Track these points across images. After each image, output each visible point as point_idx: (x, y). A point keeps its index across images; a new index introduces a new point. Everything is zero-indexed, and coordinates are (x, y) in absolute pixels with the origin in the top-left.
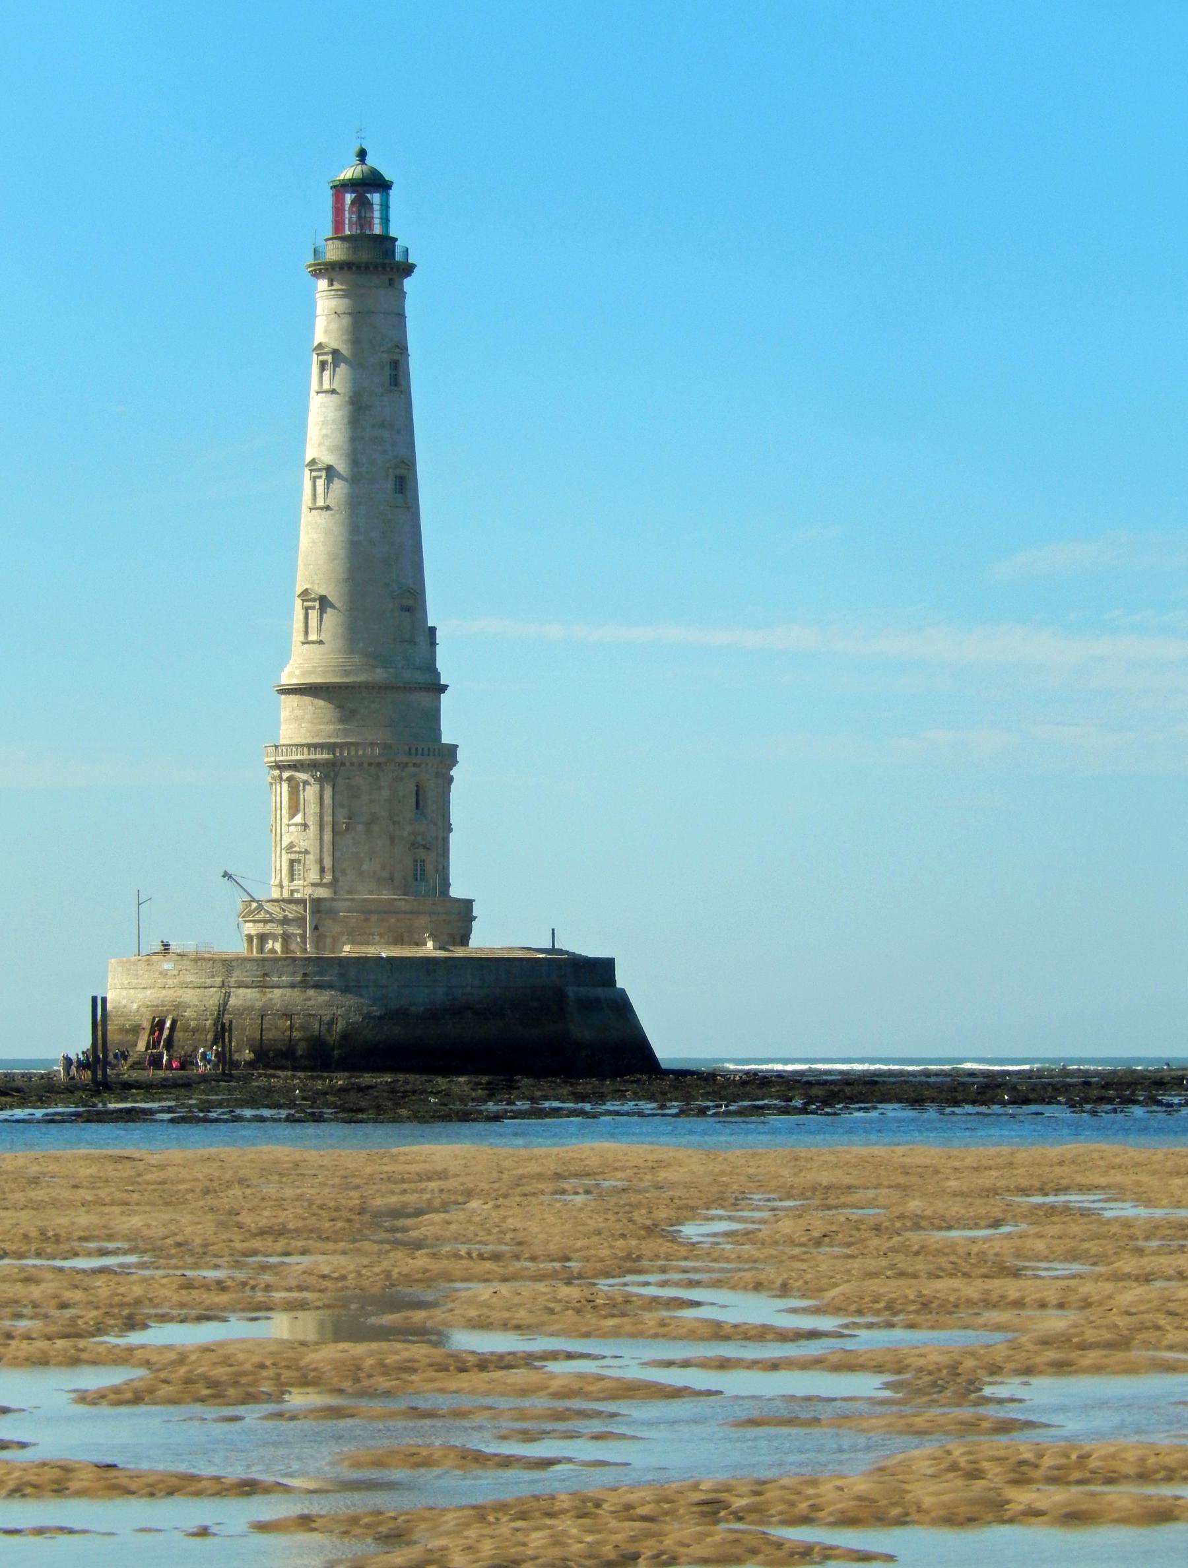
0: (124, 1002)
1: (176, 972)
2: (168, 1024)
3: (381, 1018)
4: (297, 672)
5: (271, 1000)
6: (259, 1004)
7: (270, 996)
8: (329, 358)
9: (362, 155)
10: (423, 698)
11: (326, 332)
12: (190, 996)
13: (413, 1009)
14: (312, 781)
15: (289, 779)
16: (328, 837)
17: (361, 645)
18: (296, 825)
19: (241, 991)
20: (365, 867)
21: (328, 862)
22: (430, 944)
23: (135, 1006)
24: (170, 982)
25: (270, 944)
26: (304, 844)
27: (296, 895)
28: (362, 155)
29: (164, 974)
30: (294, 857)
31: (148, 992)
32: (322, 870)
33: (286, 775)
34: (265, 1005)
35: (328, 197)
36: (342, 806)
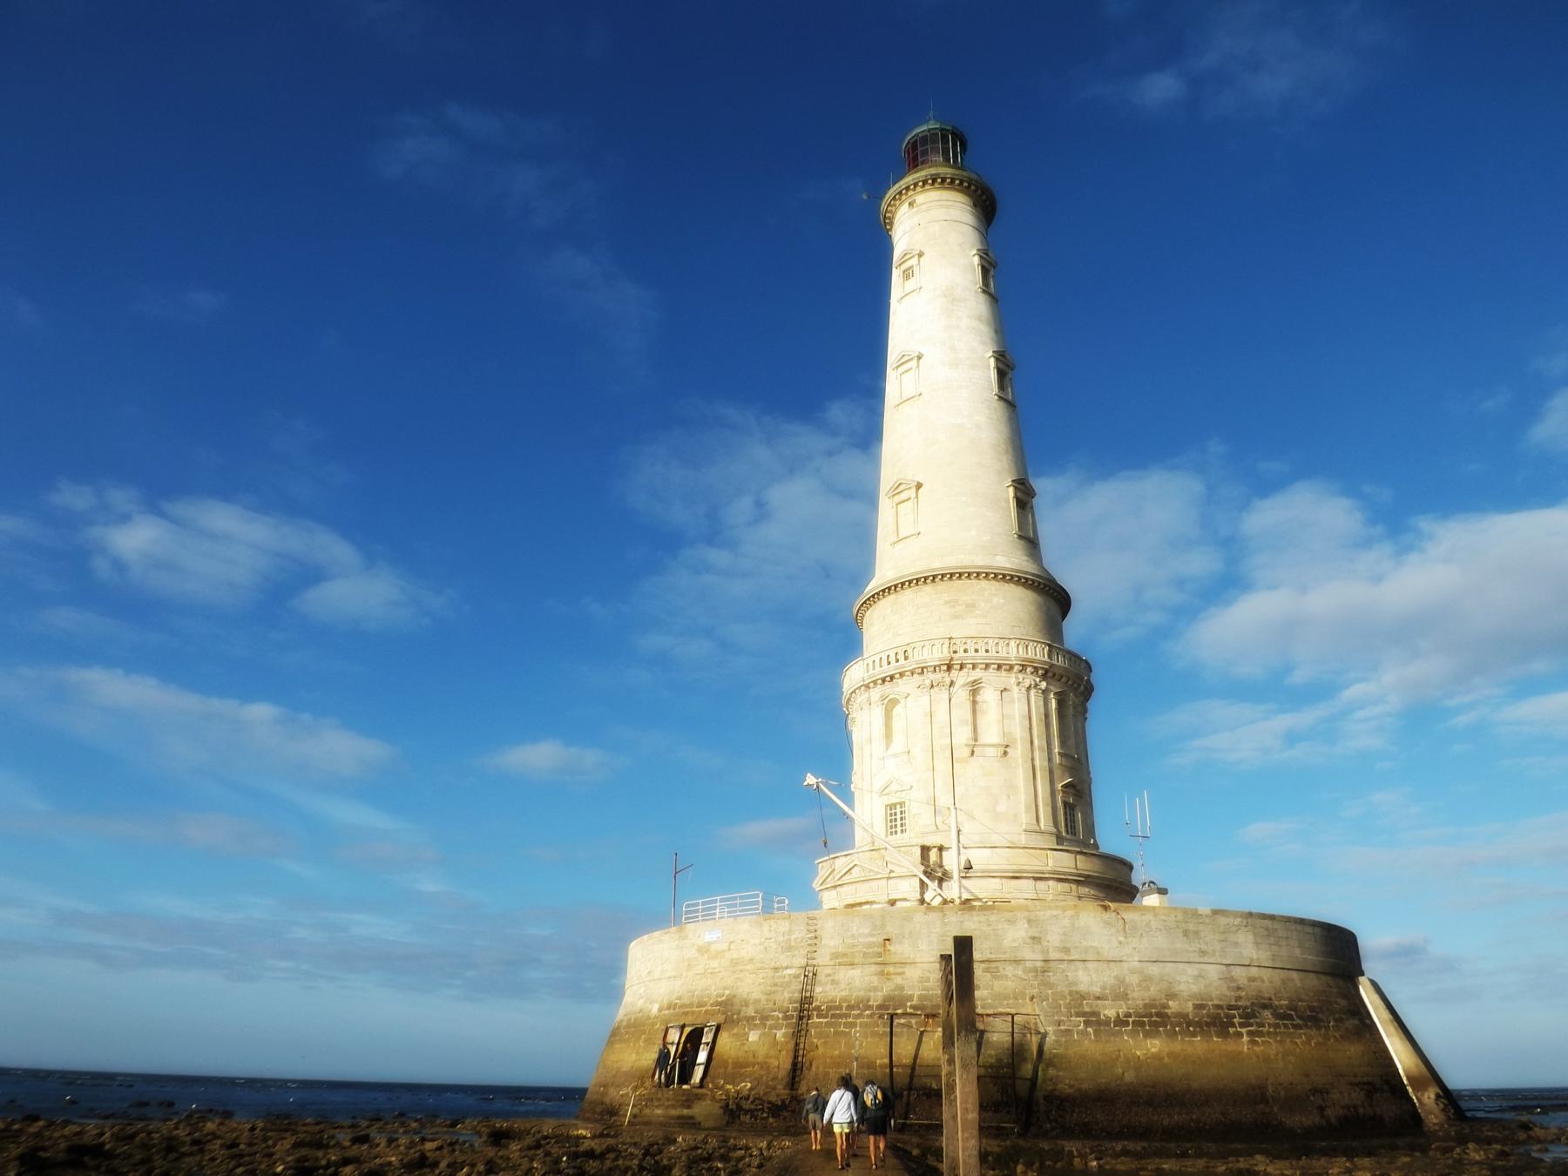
1: (725, 946)
3: (1121, 1022)
5: (902, 988)
6: (876, 999)
7: (899, 980)
12: (751, 988)
13: (1174, 1006)
16: (943, 765)
17: (973, 533)
18: (895, 756)
20: (1001, 808)
21: (944, 800)
23: (655, 1009)
24: (714, 964)
29: (704, 950)
34: (889, 998)
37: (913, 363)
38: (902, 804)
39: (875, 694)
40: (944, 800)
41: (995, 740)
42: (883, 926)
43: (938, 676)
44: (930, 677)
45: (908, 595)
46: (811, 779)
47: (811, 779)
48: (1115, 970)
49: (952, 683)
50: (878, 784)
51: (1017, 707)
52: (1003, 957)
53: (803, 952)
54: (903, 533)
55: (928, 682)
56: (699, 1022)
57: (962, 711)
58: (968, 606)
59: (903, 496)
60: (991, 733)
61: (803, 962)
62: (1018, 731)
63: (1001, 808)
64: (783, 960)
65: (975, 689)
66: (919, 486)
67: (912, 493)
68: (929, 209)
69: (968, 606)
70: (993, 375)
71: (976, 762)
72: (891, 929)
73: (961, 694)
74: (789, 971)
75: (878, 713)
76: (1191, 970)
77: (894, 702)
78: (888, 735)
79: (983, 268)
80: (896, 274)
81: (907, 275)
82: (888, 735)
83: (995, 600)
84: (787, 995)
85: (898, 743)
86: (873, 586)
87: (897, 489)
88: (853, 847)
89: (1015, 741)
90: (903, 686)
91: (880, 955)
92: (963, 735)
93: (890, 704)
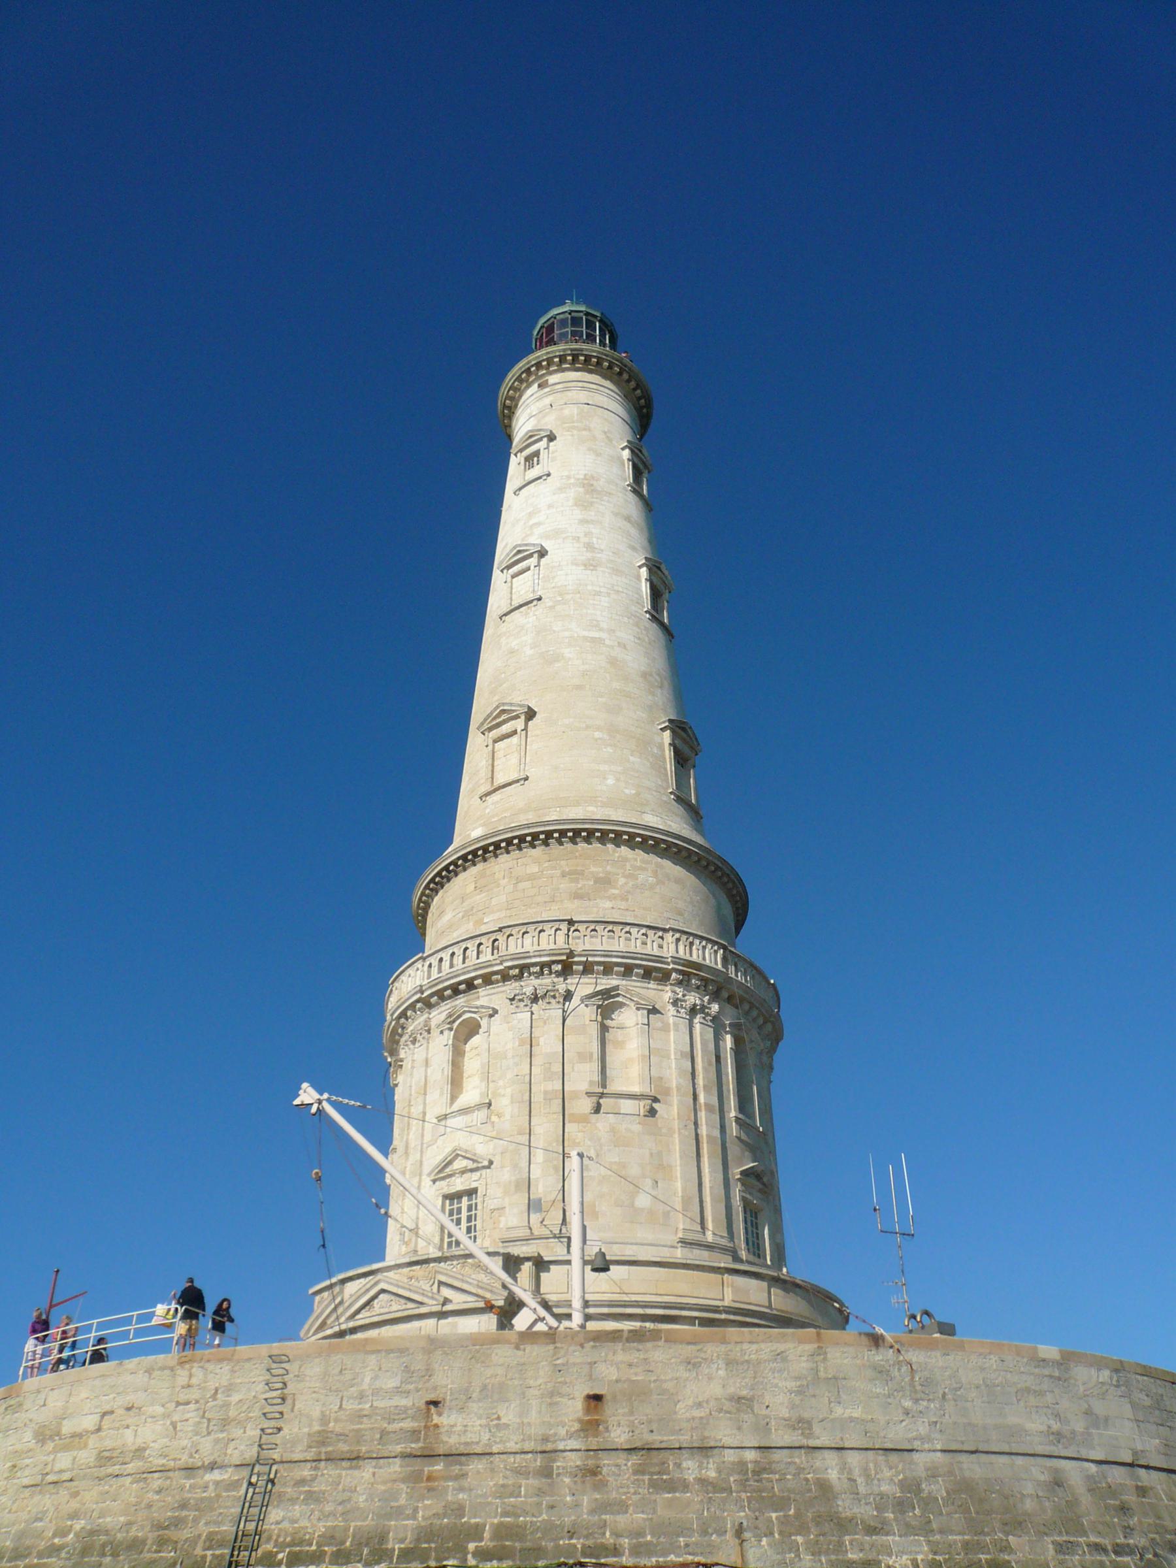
5: (460, 1510)
15: (451, 1019)
16: (545, 1127)
18: (465, 1111)
21: (545, 1186)
24: (64, 1461)
26: (482, 1148)
32: (533, 1205)
36: (583, 1057)
37: (533, 561)
38: (471, 1193)
39: (438, 1015)
40: (545, 1186)
42: (429, 1372)
43: (547, 981)
44: (529, 985)
45: (503, 863)
46: (307, 1095)
47: (307, 1095)
49: (568, 996)
52: (673, 1440)
53: (253, 1432)
54: (500, 779)
55: (529, 991)
58: (597, 880)
59: (506, 728)
61: (251, 1453)
63: (643, 1201)
64: (207, 1449)
66: (531, 714)
69: (597, 880)
70: (645, 589)
71: (602, 1123)
74: (216, 1475)
75: (439, 1046)
76: (1038, 1472)
77: (470, 1029)
79: (635, 466)
80: (515, 464)
81: (531, 460)
82: (456, 1082)
83: (641, 877)
84: (203, 1529)
85: (471, 1094)
86: (452, 852)
87: (503, 715)
88: (383, 1259)
89: (667, 1092)
90: (485, 997)
91: (414, 1434)
92: (582, 1077)
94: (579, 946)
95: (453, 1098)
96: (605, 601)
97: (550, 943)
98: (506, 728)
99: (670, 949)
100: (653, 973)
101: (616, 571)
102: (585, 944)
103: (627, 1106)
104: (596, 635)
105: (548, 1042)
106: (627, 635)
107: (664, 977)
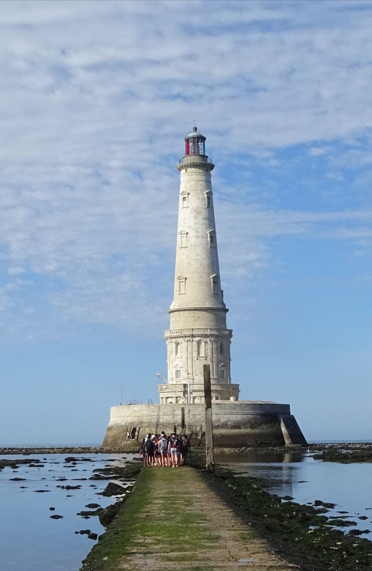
0: (119, 422)
2: (137, 429)
4: (178, 305)
6: (172, 422)
8: (186, 196)
9: (196, 129)
10: (222, 313)
11: (185, 187)
12: (145, 419)
14: (183, 342)
16: (190, 362)
19: (165, 417)
21: (190, 371)
22: (232, 399)
23: (124, 423)
25: (169, 400)
27: (178, 383)
28: (196, 129)
29: (135, 411)
30: (177, 369)
31: (129, 418)
32: (188, 374)
33: (174, 340)
35: (184, 143)
40: (190, 371)
41: (203, 356)
43: (189, 338)
44: (187, 339)
48: (219, 416)
49: (193, 341)
50: (175, 364)
51: (209, 346)
56: (135, 426)
57: (195, 348)
59: (181, 280)
60: (202, 354)
62: (209, 353)
64: (153, 414)
65: (199, 343)
67: (184, 280)
68: (192, 175)
70: (209, 239)
72: (175, 409)
73: (195, 344)
78: (177, 352)
82: (177, 352)
90: (180, 340)
92: (195, 354)
93: (177, 344)
94: (194, 333)
95: (176, 355)
96: (200, 247)
97: (189, 333)
98: (181, 280)
99: (208, 332)
100: (206, 336)
101: (203, 238)
102: (195, 333)
103: (202, 358)
104: (198, 257)
105: (190, 349)
106: (204, 256)
107: (208, 336)
